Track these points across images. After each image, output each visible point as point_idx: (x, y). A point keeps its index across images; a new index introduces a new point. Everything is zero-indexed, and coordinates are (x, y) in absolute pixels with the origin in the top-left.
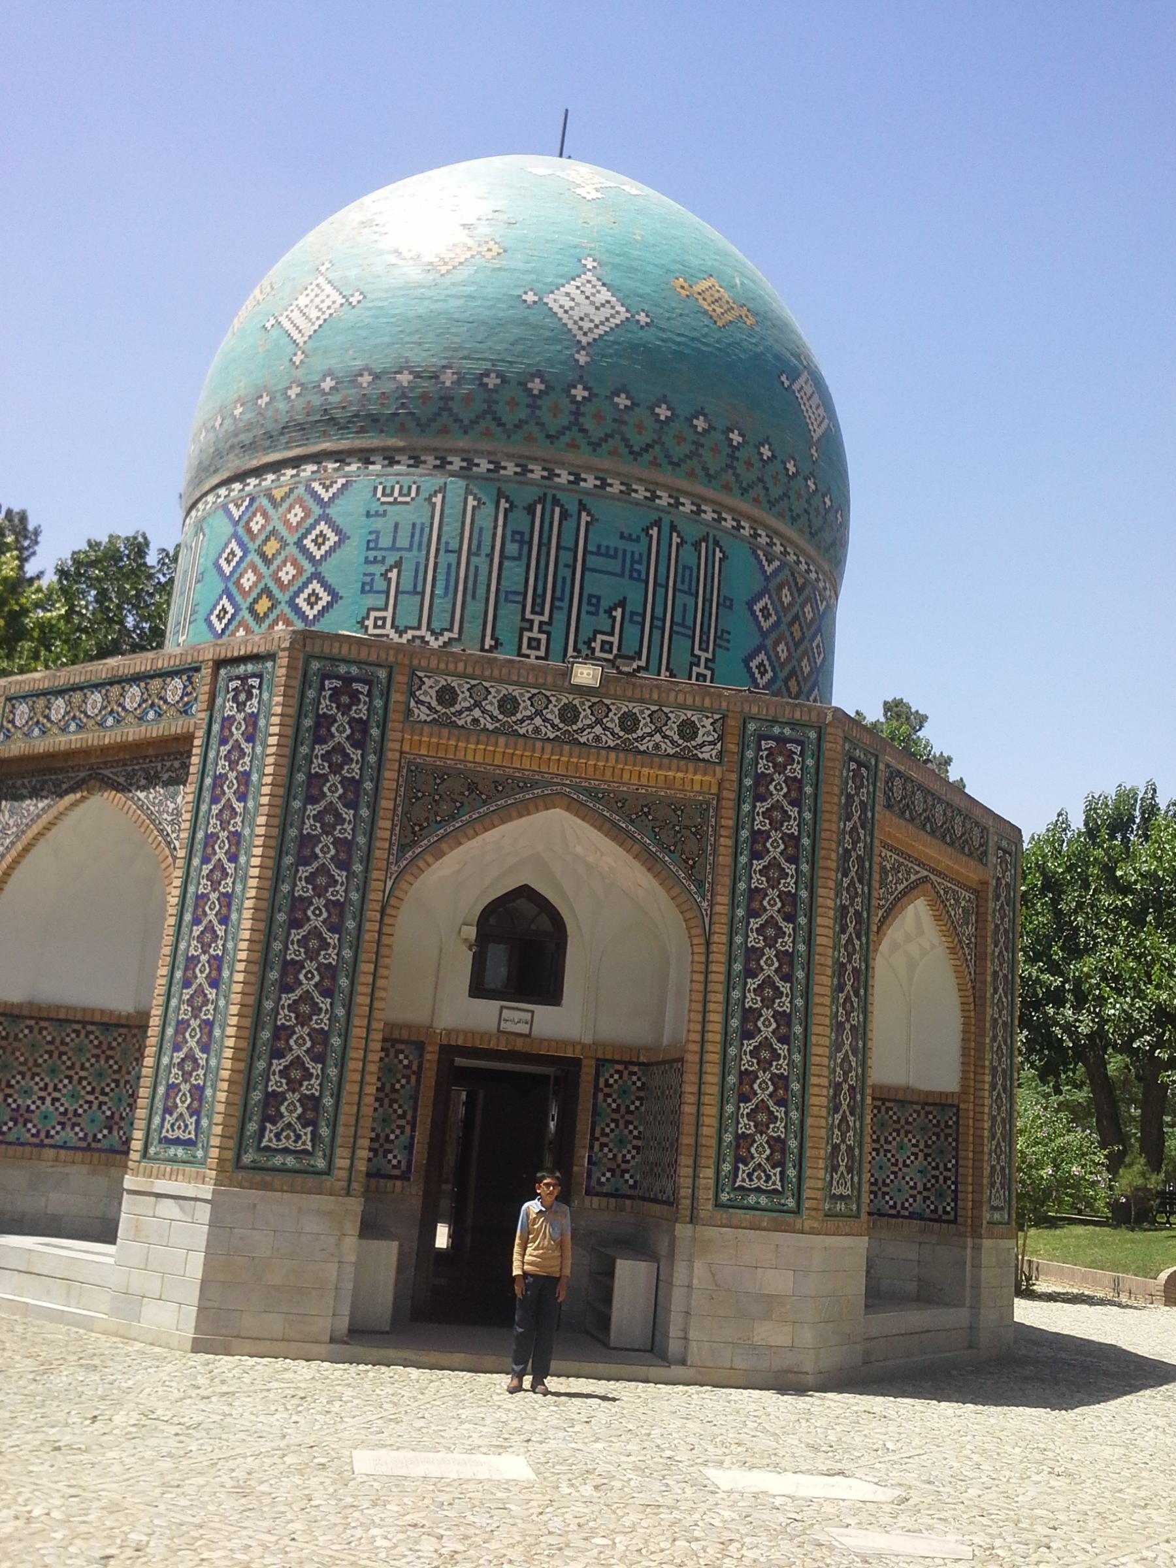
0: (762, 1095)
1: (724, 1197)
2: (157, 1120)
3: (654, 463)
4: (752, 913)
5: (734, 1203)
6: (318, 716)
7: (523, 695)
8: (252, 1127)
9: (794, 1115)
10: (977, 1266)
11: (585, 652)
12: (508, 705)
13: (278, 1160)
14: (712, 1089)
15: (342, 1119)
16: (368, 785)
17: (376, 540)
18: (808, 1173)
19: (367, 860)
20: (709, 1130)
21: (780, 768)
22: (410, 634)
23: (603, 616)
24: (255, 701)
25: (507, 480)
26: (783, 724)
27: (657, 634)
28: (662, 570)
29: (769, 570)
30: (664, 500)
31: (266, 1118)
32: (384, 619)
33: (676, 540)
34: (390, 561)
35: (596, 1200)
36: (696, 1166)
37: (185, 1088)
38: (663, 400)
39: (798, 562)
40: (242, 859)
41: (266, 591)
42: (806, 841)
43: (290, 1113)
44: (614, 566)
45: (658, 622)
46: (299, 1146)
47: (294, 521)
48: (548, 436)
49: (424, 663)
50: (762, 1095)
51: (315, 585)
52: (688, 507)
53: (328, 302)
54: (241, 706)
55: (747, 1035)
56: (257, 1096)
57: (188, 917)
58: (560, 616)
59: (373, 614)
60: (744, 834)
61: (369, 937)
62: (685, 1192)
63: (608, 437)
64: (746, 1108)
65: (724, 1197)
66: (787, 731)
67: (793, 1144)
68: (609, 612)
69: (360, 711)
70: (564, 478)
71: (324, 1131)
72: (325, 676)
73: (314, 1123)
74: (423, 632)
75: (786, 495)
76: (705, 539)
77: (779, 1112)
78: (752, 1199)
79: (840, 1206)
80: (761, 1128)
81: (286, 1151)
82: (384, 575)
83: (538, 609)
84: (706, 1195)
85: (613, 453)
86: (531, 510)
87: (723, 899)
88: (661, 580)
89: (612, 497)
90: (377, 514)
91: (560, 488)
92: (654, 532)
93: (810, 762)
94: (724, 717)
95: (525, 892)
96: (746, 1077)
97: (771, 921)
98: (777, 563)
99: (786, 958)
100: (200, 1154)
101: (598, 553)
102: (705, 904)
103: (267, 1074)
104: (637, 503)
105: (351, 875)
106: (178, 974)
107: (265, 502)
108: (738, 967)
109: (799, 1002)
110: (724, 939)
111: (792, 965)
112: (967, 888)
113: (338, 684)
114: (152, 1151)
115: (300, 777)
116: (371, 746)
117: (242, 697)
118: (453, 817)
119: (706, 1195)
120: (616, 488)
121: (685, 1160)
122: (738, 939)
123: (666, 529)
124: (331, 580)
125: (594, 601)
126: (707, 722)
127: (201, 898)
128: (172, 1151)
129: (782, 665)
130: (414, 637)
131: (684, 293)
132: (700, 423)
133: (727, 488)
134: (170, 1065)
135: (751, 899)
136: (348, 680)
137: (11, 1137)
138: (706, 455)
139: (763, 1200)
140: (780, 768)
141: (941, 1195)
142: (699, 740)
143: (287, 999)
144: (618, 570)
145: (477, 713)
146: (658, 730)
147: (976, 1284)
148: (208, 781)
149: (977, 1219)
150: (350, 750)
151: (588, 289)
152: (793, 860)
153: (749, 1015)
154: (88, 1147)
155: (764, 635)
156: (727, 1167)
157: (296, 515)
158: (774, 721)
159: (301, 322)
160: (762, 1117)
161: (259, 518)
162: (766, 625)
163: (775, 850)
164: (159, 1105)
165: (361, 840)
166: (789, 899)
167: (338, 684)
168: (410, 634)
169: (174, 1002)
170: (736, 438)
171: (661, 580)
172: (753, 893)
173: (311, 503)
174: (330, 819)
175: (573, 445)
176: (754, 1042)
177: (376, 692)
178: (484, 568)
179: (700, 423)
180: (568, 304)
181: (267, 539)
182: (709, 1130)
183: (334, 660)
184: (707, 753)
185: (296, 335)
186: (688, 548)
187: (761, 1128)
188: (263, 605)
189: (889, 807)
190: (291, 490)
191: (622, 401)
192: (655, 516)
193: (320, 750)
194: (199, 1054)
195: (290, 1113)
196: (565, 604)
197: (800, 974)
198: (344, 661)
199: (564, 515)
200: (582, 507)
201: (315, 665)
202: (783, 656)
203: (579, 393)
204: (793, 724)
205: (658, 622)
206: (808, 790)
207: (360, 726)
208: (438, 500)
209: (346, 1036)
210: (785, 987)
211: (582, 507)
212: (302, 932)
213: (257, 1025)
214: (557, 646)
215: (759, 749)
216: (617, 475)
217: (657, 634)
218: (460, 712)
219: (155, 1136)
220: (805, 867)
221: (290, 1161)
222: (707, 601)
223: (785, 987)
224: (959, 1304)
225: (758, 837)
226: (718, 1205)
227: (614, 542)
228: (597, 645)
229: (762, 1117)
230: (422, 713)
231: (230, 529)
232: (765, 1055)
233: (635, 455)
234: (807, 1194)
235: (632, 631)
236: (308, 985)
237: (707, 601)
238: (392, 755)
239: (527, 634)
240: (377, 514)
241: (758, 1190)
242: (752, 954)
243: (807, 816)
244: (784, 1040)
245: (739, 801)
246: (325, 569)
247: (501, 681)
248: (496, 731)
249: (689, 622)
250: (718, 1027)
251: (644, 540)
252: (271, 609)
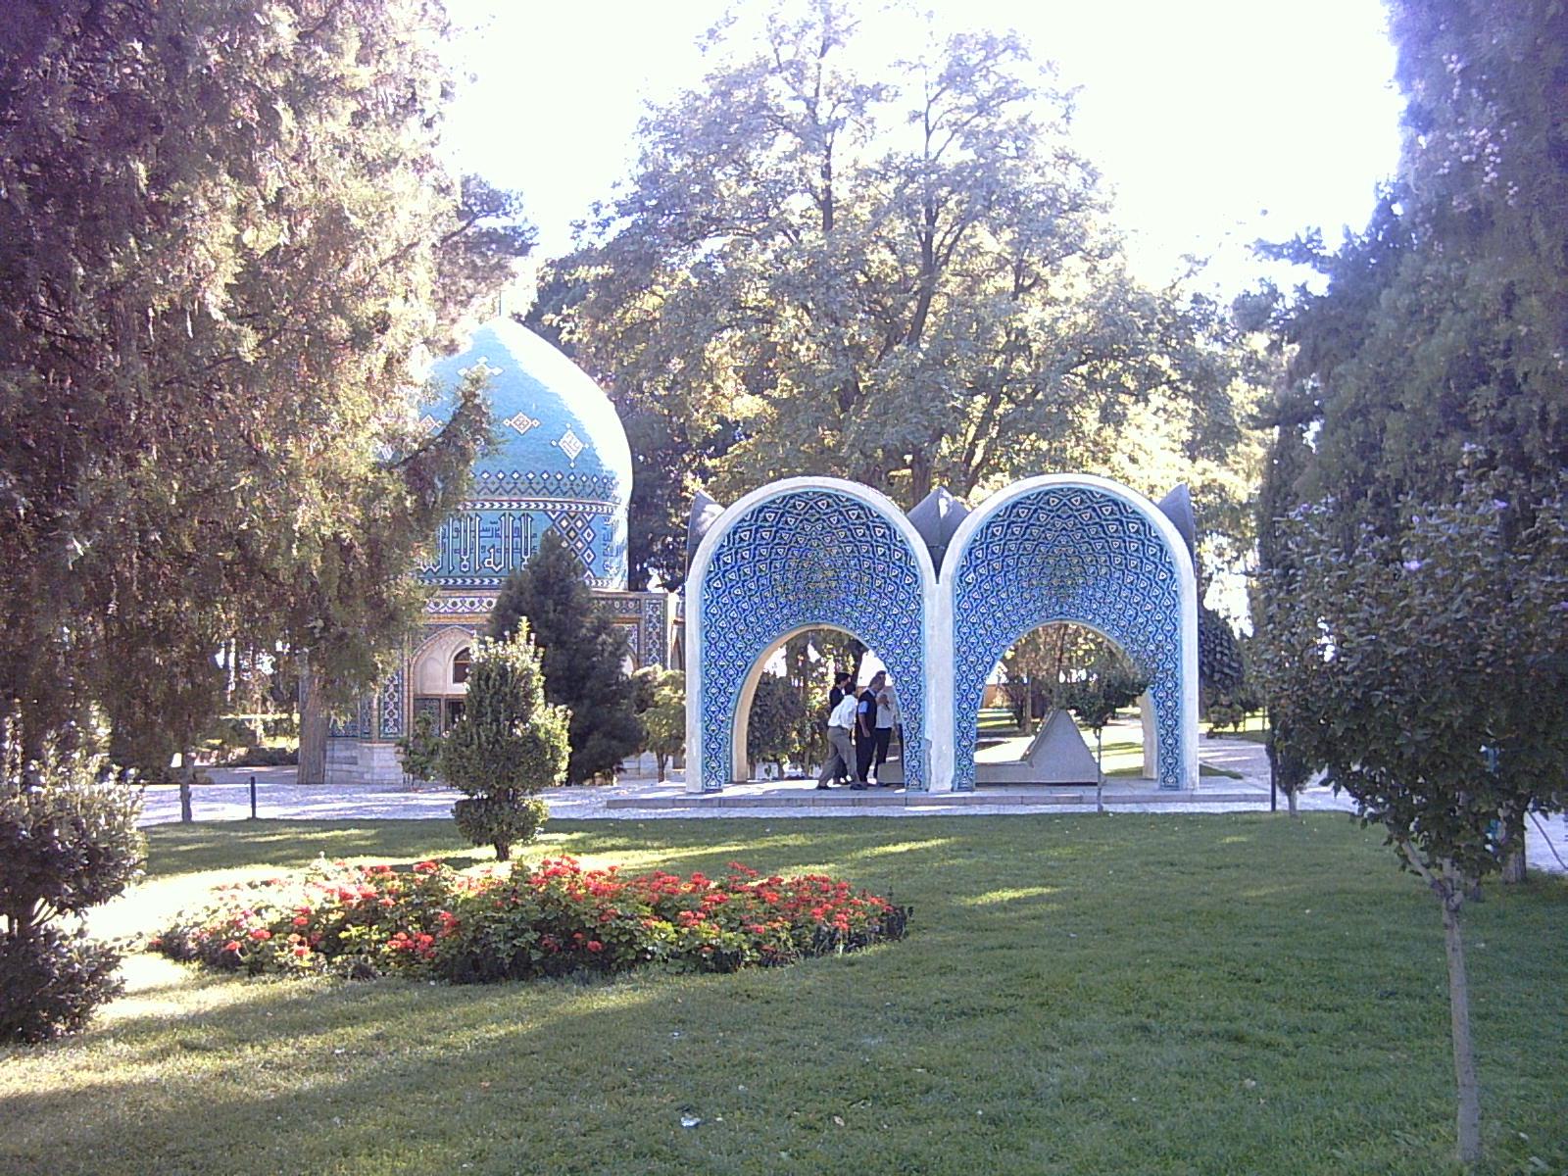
30: (506, 505)
43: (391, 724)
52: (515, 505)
138: (519, 485)
170: (531, 476)
179: (516, 476)
191: (485, 475)
195: (391, 724)
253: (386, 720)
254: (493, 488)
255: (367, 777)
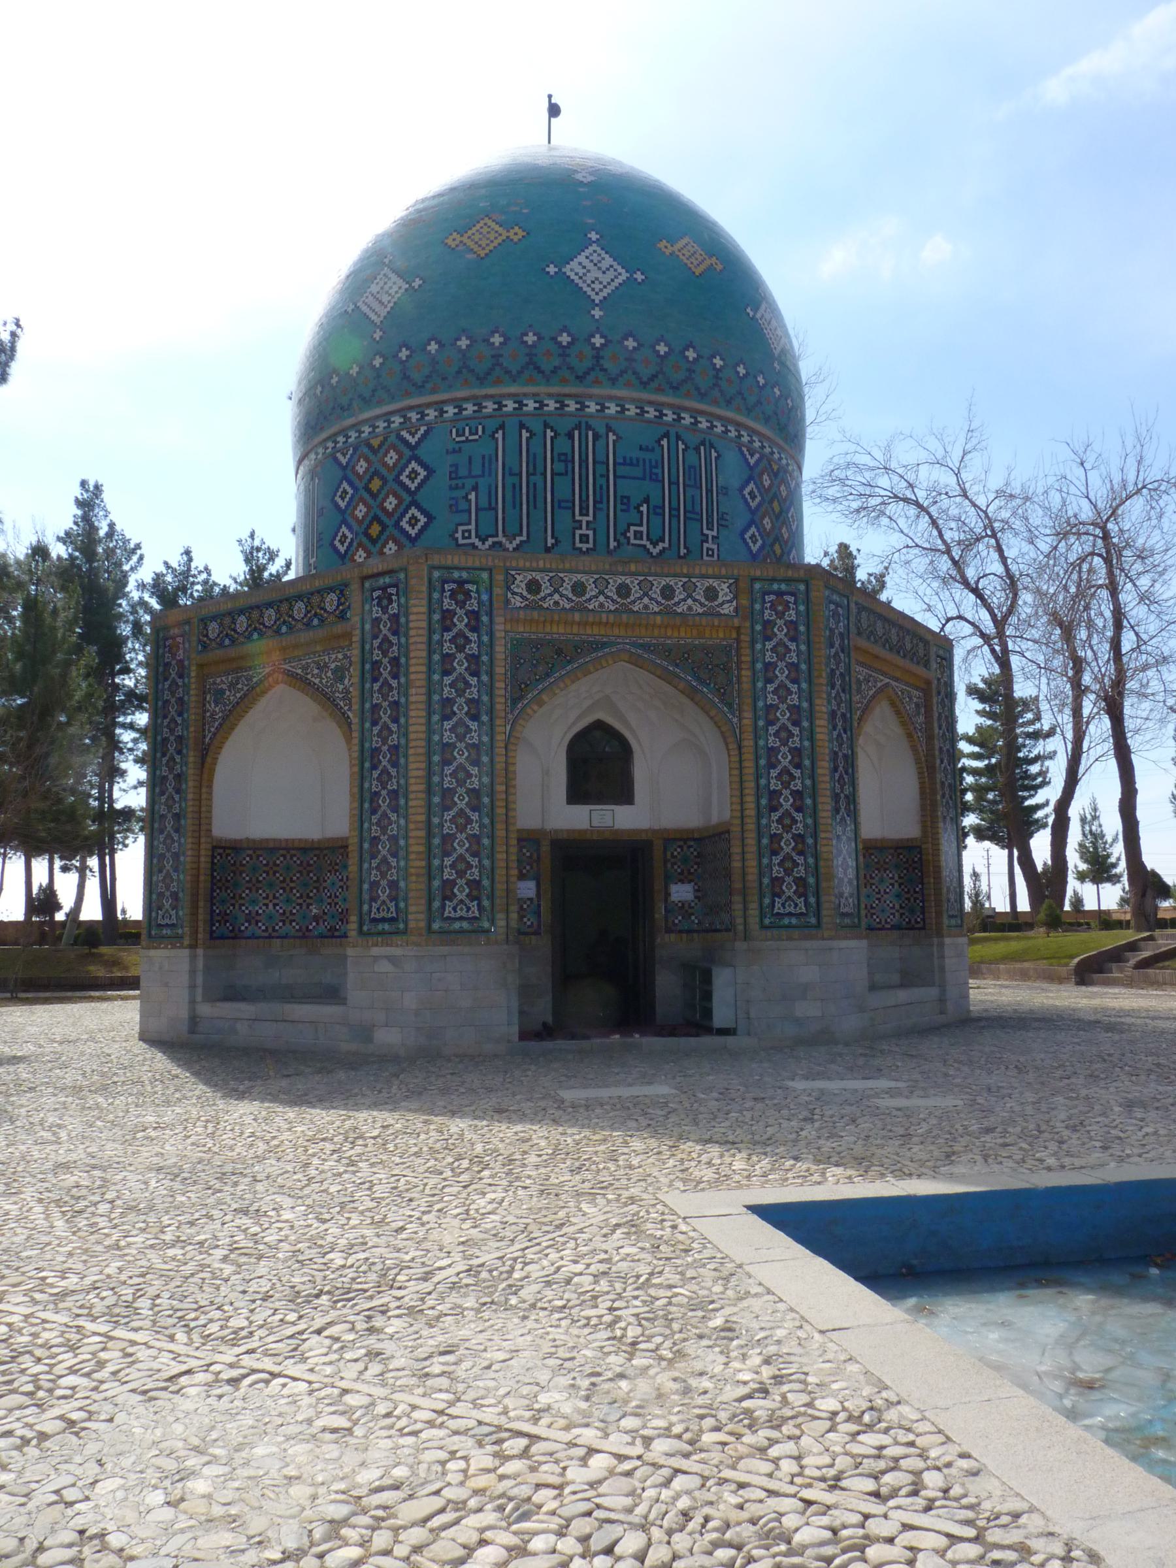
0: (787, 849)
1: (767, 921)
2: (366, 907)
3: (659, 390)
4: (771, 723)
5: (774, 924)
6: (443, 612)
7: (588, 580)
8: (436, 904)
9: (811, 861)
10: (942, 957)
11: (623, 540)
12: (579, 589)
13: (457, 925)
14: (752, 848)
15: (497, 893)
16: (485, 658)
17: (456, 472)
18: (823, 899)
19: (491, 712)
20: (752, 877)
21: (780, 615)
22: (491, 541)
23: (633, 512)
24: (395, 605)
25: (550, 414)
26: (780, 581)
27: (674, 521)
28: (674, 470)
29: (752, 461)
30: (670, 417)
31: (445, 898)
32: (469, 531)
33: (681, 446)
34: (468, 486)
35: (673, 936)
36: (745, 902)
37: (384, 883)
38: (661, 339)
39: (772, 453)
40: (402, 720)
41: (376, 518)
42: (803, 667)
44: (637, 471)
45: (674, 510)
46: (470, 915)
47: (391, 463)
48: (577, 377)
49: (514, 564)
50: (787, 849)
51: (413, 511)
53: (395, 288)
54: (385, 610)
55: (773, 809)
56: (436, 883)
57: (367, 765)
58: (601, 516)
59: (461, 528)
60: (759, 666)
61: (500, 766)
62: (739, 921)
63: (623, 372)
64: (776, 860)
65: (767, 921)
66: (783, 587)
67: (811, 880)
68: (637, 508)
69: (472, 604)
70: (593, 407)
71: (486, 903)
72: (445, 582)
73: (478, 899)
74: (501, 538)
75: (759, 403)
76: (703, 443)
77: (800, 860)
78: (786, 921)
79: (847, 921)
80: (788, 872)
81: (461, 918)
82: (466, 497)
83: (584, 511)
84: (754, 921)
85: (628, 385)
86: (570, 436)
87: (748, 714)
88: (674, 479)
89: (631, 419)
90: (454, 451)
91: (591, 416)
92: (664, 442)
93: (802, 608)
94: (737, 580)
95: (599, 725)
96: (775, 838)
97: (783, 727)
98: (757, 456)
99: (797, 752)
100: (401, 926)
101: (624, 464)
102: (735, 720)
103: (441, 868)
104: (649, 421)
105: (481, 724)
106: (366, 805)
107: (366, 450)
108: (762, 762)
109: (808, 782)
110: (752, 743)
111: (800, 756)
112: (917, 688)
113: (454, 586)
114: (365, 928)
115: (436, 657)
116: (484, 630)
117: (385, 602)
118: (548, 675)
119: (754, 921)
120: (632, 411)
121: (737, 898)
122: (761, 743)
123: (673, 439)
124: (425, 505)
125: (625, 501)
126: (725, 586)
127: (375, 751)
128: (380, 927)
129: (768, 534)
130: (494, 543)
131: (668, 252)
132: (691, 354)
133: (715, 402)
134: (370, 868)
135: (767, 713)
136: (461, 583)
137: (248, 933)
139: (794, 921)
140: (780, 615)
141: (912, 911)
142: (720, 600)
143: (448, 816)
144: (640, 475)
145: (556, 597)
146: (690, 596)
147: (942, 969)
148: (368, 666)
149: (939, 924)
150: (469, 634)
151: (595, 258)
152: (795, 681)
153: (774, 795)
154: (304, 935)
155: (753, 512)
156: (767, 901)
157: (391, 458)
158: (773, 580)
159: (376, 305)
160: (788, 864)
161: (363, 463)
162: (753, 505)
163: (782, 675)
164: (366, 897)
165: (485, 698)
166: (795, 709)
167: (454, 586)
168: (491, 541)
169: (366, 825)
170: (718, 362)
171: (674, 479)
172: (769, 708)
173: (402, 447)
174: (461, 686)
175: (597, 382)
176: (778, 814)
177: (482, 589)
178: (540, 485)
179: (691, 354)
180: (581, 271)
181: (371, 479)
182: (752, 877)
183: (448, 568)
184: (727, 609)
185: (373, 317)
186: (691, 452)
187: (788, 872)
188: (375, 530)
189: (859, 634)
190: (386, 439)
191: (631, 343)
192: (663, 430)
193: (447, 636)
194: (390, 859)
196: (604, 506)
197: (807, 762)
198: (457, 568)
199: (596, 437)
200: (609, 429)
201: (436, 574)
202: (768, 527)
203: (598, 341)
204: (788, 581)
205: (674, 510)
206: (802, 628)
207: (474, 615)
208: (499, 435)
209: (492, 837)
210: (797, 773)
211: (609, 429)
212: (452, 768)
213: (430, 835)
214: (601, 539)
215: (764, 602)
216: (633, 401)
217: (674, 521)
218: (544, 598)
219: (366, 918)
220: (804, 686)
221: (465, 925)
222: (709, 491)
223: (797, 773)
224: (933, 985)
225: (769, 666)
226: (763, 927)
227: (635, 454)
228: (631, 535)
229: (788, 864)
230: (517, 602)
231: (340, 473)
232: (787, 822)
233: (644, 384)
234: (824, 912)
235: (656, 520)
236: (462, 805)
237: (709, 491)
238: (499, 635)
239: (578, 532)
240: (454, 451)
241: (790, 914)
242: (772, 751)
243: (803, 648)
244: (799, 809)
245: (753, 642)
246: (418, 497)
247: (571, 571)
248: (572, 609)
249: (698, 509)
250: (752, 806)
251: (658, 450)
252: (381, 532)
253: (449, 884)
254: (646, 372)
255: (388, 1037)
